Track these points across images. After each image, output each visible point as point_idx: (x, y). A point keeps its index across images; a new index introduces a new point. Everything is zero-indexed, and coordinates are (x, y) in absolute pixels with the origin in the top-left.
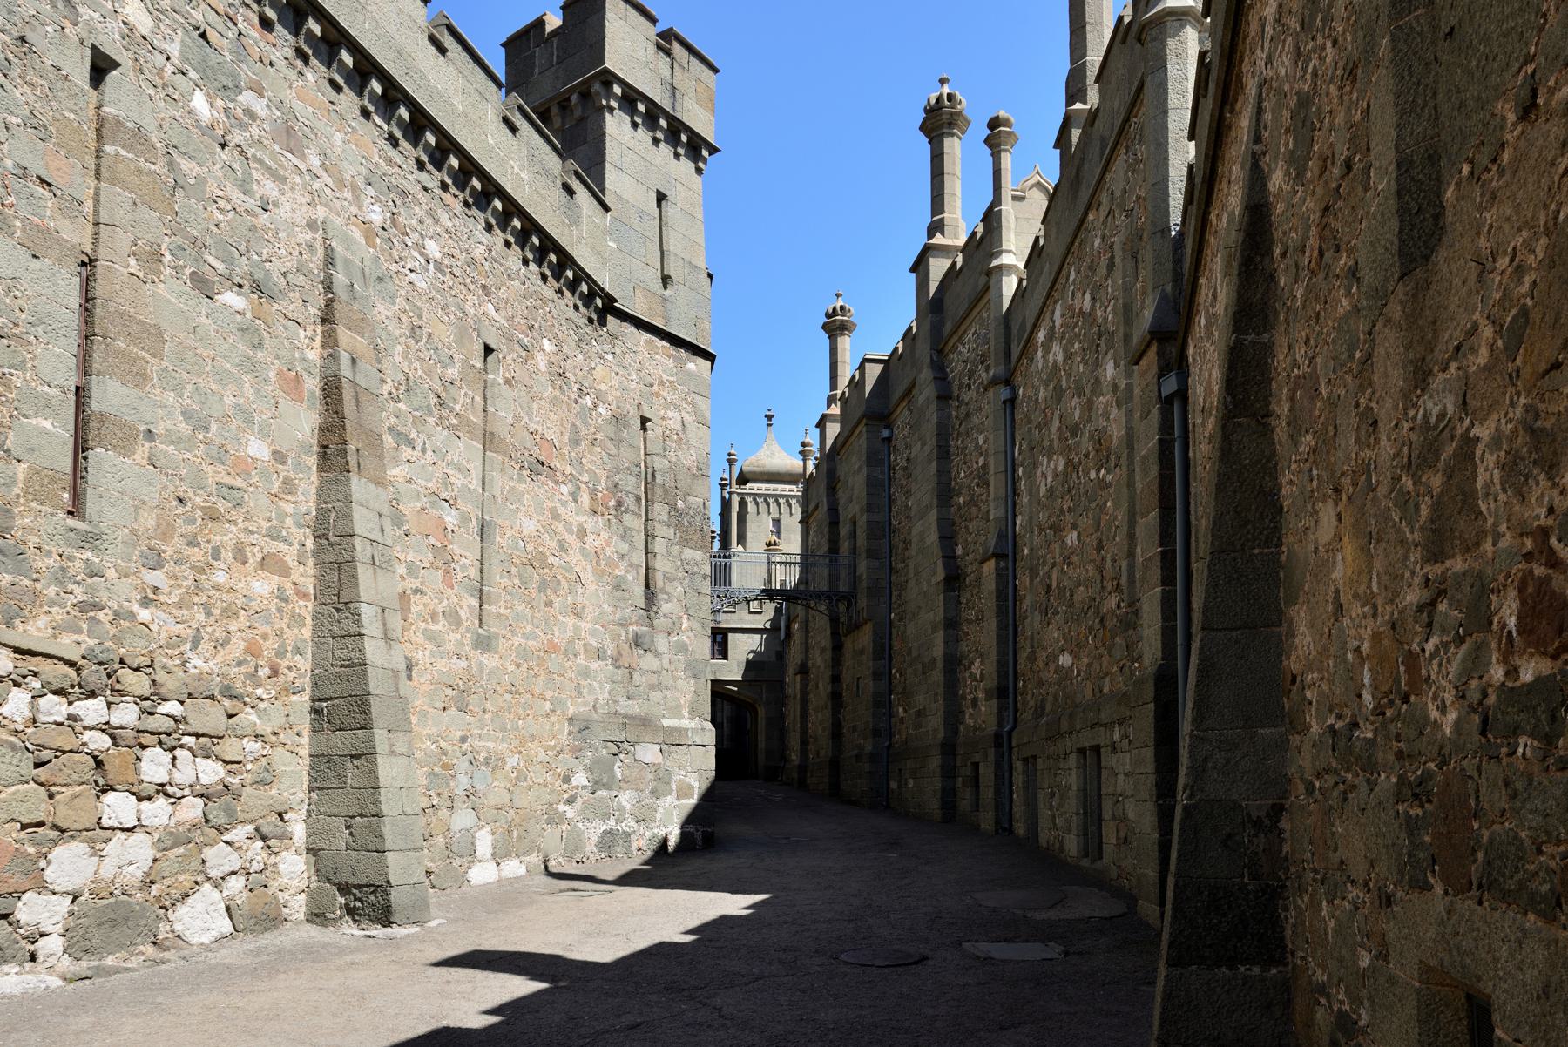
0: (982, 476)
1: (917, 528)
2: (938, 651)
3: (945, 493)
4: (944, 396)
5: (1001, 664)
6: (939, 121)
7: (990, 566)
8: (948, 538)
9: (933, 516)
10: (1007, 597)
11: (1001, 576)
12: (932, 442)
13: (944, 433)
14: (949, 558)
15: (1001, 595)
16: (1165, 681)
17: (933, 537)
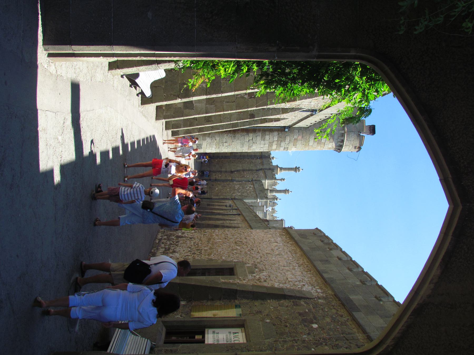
0: (243, 177)
1: (241, 165)
2: (223, 170)
3: (244, 170)
4: (257, 170)
5: (219, 180)
6: (296, 169)
7: (230, 178)
8: (237, 171)
9: (241, 169)
10: (227, 180)
11: (229, 180)
12: (251, 168)
13: (252, 170)
14: (235, 171)
15: (227, 180)
16: (211, 198)
17: (238, 169)
